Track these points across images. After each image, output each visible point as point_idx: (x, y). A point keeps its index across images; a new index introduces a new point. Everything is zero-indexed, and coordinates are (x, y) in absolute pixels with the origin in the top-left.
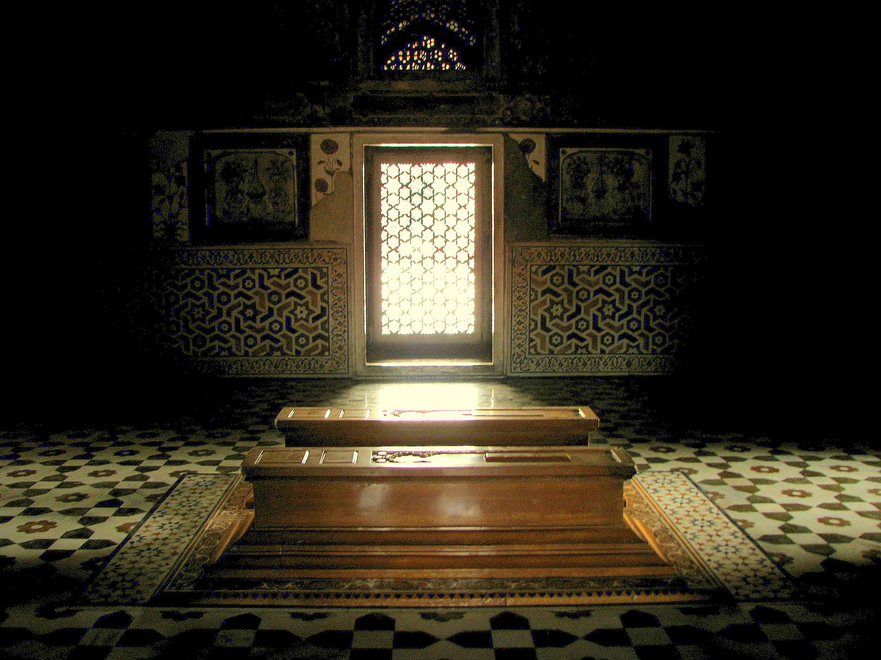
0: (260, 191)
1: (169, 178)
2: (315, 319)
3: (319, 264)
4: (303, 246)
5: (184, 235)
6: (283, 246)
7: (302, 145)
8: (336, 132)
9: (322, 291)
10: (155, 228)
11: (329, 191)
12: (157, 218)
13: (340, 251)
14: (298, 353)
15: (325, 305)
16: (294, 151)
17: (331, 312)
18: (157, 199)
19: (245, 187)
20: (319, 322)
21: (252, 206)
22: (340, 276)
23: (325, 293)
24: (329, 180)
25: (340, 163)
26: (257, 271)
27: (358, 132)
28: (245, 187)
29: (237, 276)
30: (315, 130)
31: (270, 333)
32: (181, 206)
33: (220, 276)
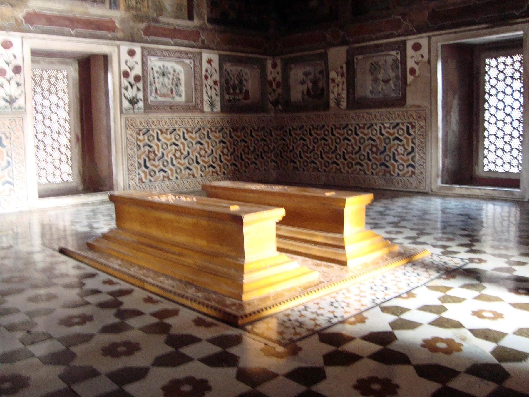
0: (388, 78)
1: (337, 73)
2: (408, 154)
3: (411, 120)
4: (403, 109)
5: (344, 105)
6: (389, 110)
7: (402, 47)
8: (421, 38)
9: (412, 137)
10: (331, 101)
11: (417, 75)
12: (332, 96)
13: (422, 112)
14: (398, 174)
15: (413, 146)
16: (399, 52)
17: (417, 150)
18: (331, 85)
19: (380, 76)
20: (410, 157)
21: (384, 87)
22: (422, 127)
23: (414, 138)
24: (416, 67)
25: (422, 56)
26: (378, 125)
27: (434, 36)
28: (380, 76)
29: (368, 128)
30: (409, 37)
31: (384, 162)
32: (343, 89)
33: (360, 128)
